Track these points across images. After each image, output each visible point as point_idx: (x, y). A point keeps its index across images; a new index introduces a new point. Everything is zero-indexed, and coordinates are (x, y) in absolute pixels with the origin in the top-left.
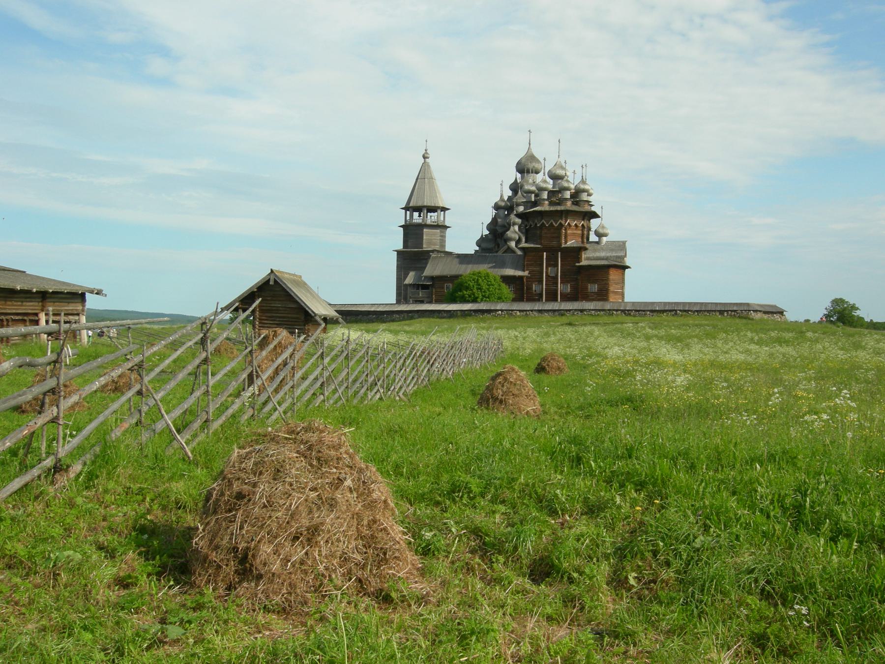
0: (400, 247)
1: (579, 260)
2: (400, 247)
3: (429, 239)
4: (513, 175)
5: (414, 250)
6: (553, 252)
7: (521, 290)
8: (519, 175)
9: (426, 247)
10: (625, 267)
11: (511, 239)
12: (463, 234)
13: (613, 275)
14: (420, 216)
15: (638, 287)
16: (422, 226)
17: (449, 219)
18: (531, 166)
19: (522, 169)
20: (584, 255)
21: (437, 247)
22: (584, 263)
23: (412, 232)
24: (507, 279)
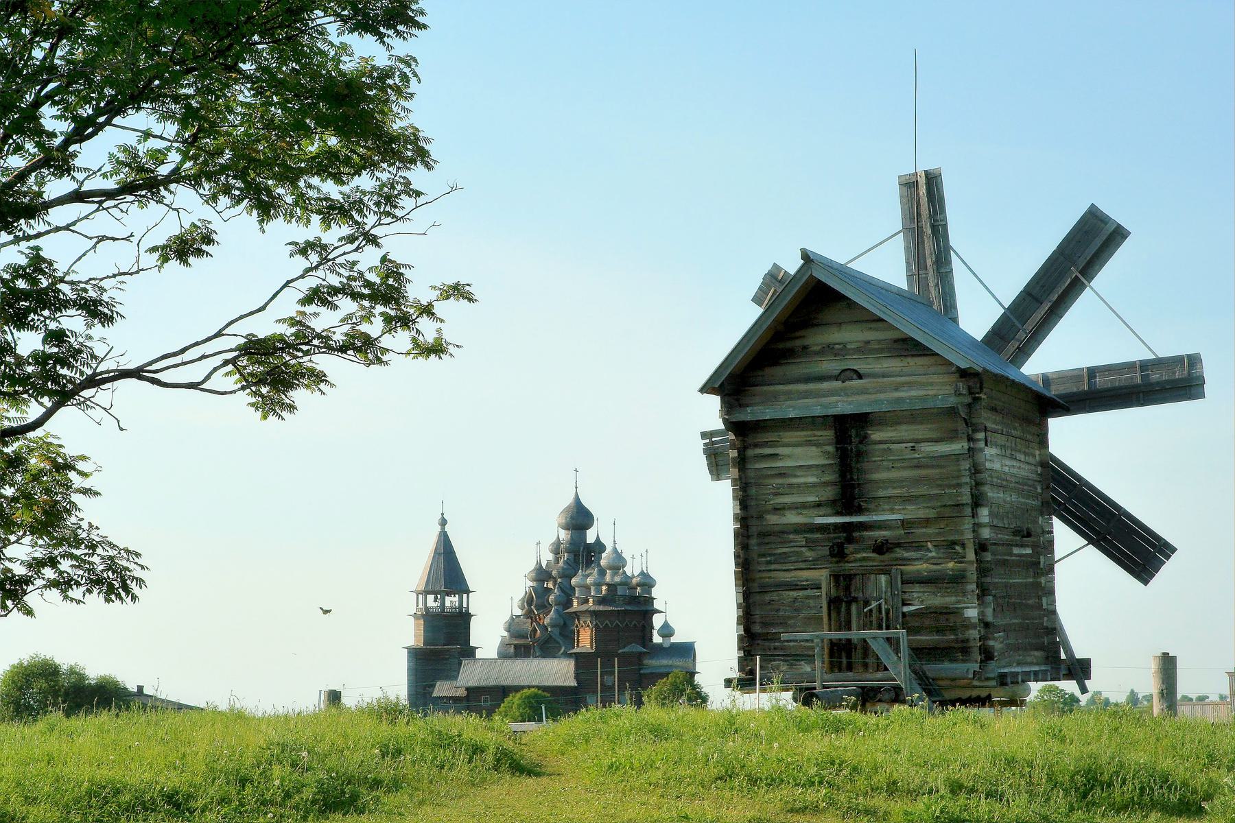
14: (435, 601)
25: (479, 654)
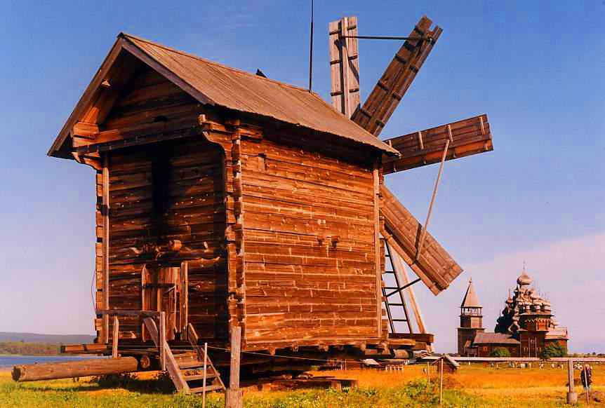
1: (544, 336)
2: (460, 327)
3: (474, 323)
4: (516, 285)
5: (466, 331)
8: (519, 286)
9: (472, 327)
11: (515, 321)
12: (489, 323)
16: (469, 317)
18: (525, 281)
19: (519, 282)
21: (478, 327)
23: (465, 320)
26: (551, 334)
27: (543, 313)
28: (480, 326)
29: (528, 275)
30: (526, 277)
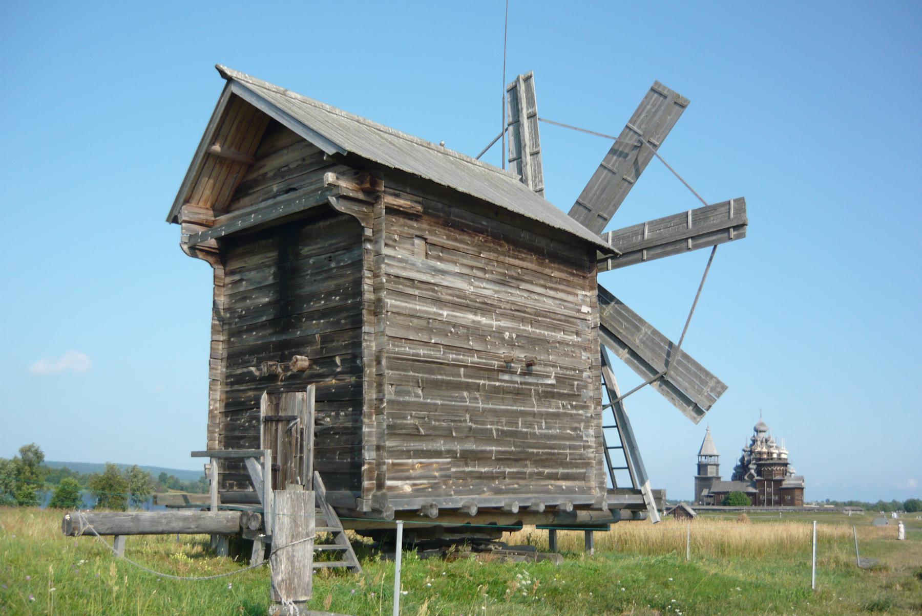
0: (696, 475)
2: (696, 475)
3: (711, 471)
4: (752, 433)
5: (703, 479)
6: (770, 481)
7: (756, 500)
9: (709, 475)
10: (802, 489)
12: (726, 473)
13: (797, 492)
15: (810, 497)
16: (706, 465)
17: (720, 461)
18: (762, 428)
19: (757, 431)
20: (784, 483)
21: (715, 475)
22: (784, 486)
23: (702, 467)
24: (749, 494)
25: (722, 479)
26: (788, 483)
27: (780, 462)
28: (717, 473)
29: (765, 422)
30: (762, 424)
